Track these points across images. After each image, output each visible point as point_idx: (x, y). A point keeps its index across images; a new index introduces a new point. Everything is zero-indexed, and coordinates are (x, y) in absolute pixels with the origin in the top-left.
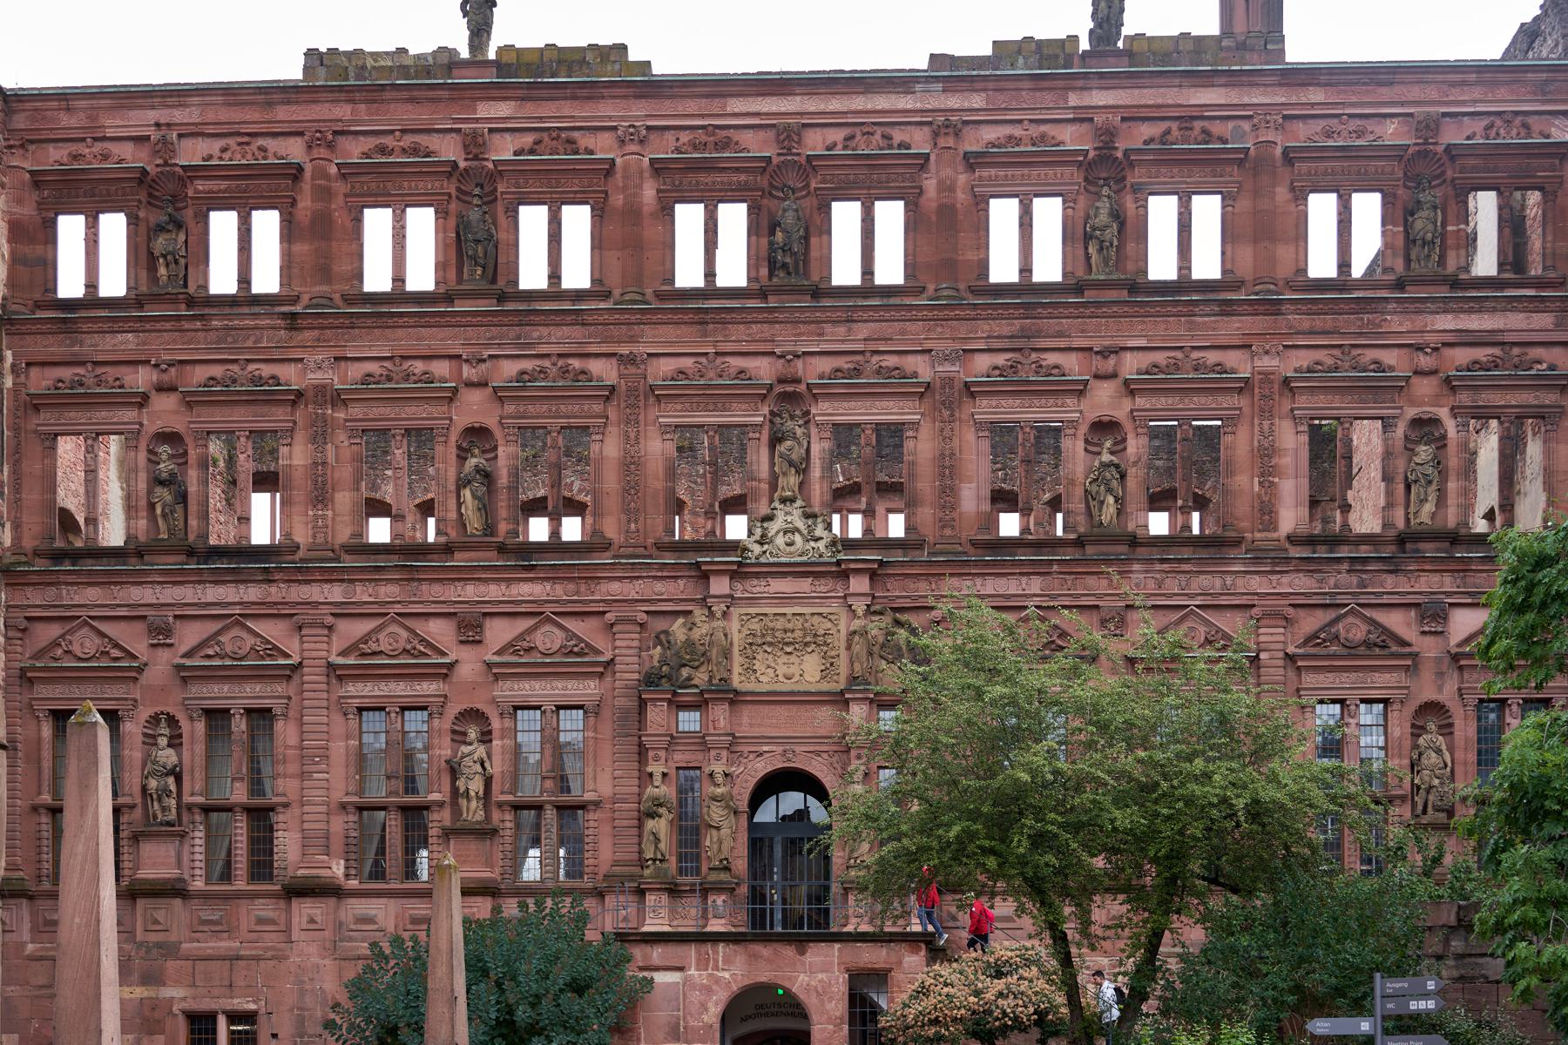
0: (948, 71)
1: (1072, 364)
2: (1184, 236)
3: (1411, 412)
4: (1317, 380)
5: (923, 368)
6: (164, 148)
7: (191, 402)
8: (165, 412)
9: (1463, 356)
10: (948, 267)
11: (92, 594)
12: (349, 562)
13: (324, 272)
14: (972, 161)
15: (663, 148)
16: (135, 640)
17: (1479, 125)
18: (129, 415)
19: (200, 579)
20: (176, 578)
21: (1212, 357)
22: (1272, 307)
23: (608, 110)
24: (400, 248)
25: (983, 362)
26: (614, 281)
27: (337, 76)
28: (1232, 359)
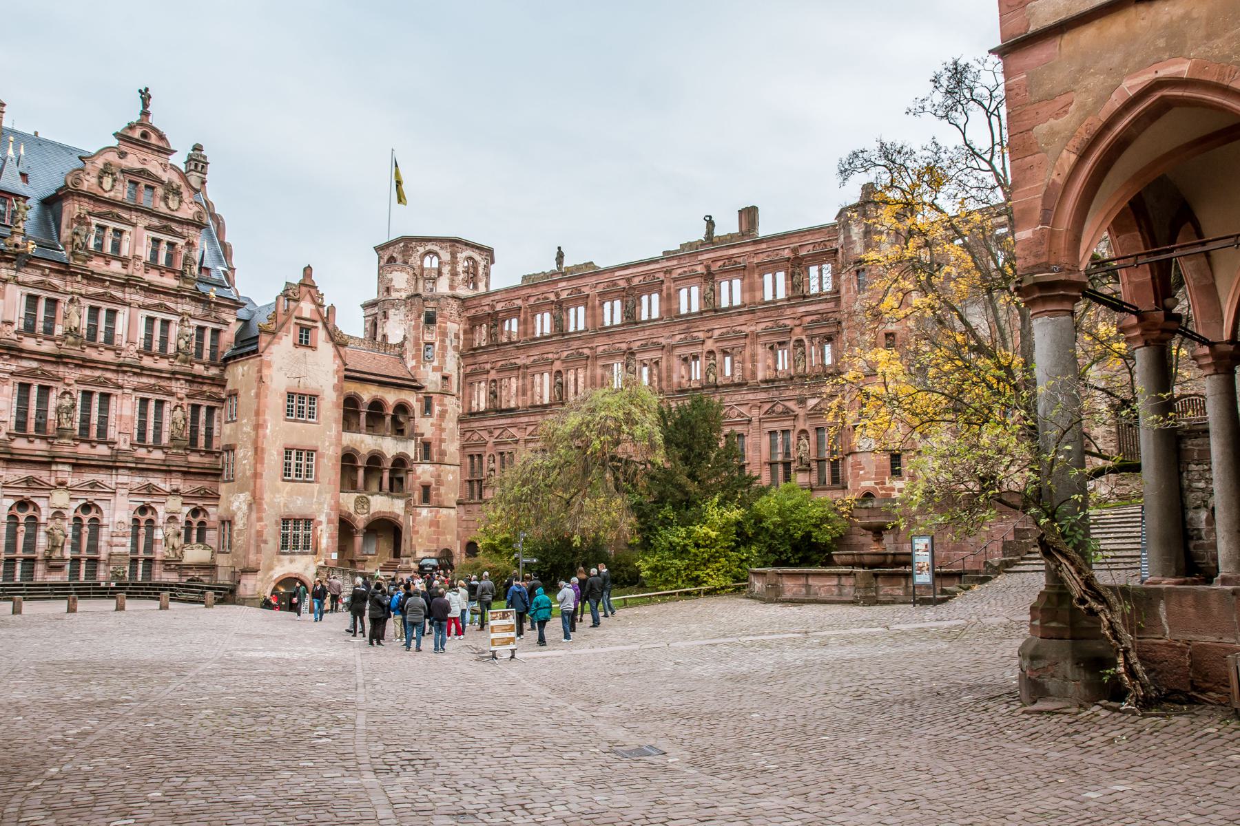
0: (669, 256)
1: (701, 335)
2: (731, 292)
3: (794, 338)
4: (766, 332)
5: (663, 341)
6: (493, 307)
7: (499, 371)
8: (493, 375)
9: (809, 319)
10: (669, 311)
11: (476, 424)
12: (531, 410)
13: (525, 334)
14: (675, 280)
15: (600, 289)
16: (485, 435)
17: (810, 247)
19: (498, 418)
20: (493, 418)
21: (738, 328)
22: (753, 312)
23: (587, 281)
24: (544, 324)
25: (678, 337)
26: (589, 327)
27: (531, 282)
28: (743, 328)
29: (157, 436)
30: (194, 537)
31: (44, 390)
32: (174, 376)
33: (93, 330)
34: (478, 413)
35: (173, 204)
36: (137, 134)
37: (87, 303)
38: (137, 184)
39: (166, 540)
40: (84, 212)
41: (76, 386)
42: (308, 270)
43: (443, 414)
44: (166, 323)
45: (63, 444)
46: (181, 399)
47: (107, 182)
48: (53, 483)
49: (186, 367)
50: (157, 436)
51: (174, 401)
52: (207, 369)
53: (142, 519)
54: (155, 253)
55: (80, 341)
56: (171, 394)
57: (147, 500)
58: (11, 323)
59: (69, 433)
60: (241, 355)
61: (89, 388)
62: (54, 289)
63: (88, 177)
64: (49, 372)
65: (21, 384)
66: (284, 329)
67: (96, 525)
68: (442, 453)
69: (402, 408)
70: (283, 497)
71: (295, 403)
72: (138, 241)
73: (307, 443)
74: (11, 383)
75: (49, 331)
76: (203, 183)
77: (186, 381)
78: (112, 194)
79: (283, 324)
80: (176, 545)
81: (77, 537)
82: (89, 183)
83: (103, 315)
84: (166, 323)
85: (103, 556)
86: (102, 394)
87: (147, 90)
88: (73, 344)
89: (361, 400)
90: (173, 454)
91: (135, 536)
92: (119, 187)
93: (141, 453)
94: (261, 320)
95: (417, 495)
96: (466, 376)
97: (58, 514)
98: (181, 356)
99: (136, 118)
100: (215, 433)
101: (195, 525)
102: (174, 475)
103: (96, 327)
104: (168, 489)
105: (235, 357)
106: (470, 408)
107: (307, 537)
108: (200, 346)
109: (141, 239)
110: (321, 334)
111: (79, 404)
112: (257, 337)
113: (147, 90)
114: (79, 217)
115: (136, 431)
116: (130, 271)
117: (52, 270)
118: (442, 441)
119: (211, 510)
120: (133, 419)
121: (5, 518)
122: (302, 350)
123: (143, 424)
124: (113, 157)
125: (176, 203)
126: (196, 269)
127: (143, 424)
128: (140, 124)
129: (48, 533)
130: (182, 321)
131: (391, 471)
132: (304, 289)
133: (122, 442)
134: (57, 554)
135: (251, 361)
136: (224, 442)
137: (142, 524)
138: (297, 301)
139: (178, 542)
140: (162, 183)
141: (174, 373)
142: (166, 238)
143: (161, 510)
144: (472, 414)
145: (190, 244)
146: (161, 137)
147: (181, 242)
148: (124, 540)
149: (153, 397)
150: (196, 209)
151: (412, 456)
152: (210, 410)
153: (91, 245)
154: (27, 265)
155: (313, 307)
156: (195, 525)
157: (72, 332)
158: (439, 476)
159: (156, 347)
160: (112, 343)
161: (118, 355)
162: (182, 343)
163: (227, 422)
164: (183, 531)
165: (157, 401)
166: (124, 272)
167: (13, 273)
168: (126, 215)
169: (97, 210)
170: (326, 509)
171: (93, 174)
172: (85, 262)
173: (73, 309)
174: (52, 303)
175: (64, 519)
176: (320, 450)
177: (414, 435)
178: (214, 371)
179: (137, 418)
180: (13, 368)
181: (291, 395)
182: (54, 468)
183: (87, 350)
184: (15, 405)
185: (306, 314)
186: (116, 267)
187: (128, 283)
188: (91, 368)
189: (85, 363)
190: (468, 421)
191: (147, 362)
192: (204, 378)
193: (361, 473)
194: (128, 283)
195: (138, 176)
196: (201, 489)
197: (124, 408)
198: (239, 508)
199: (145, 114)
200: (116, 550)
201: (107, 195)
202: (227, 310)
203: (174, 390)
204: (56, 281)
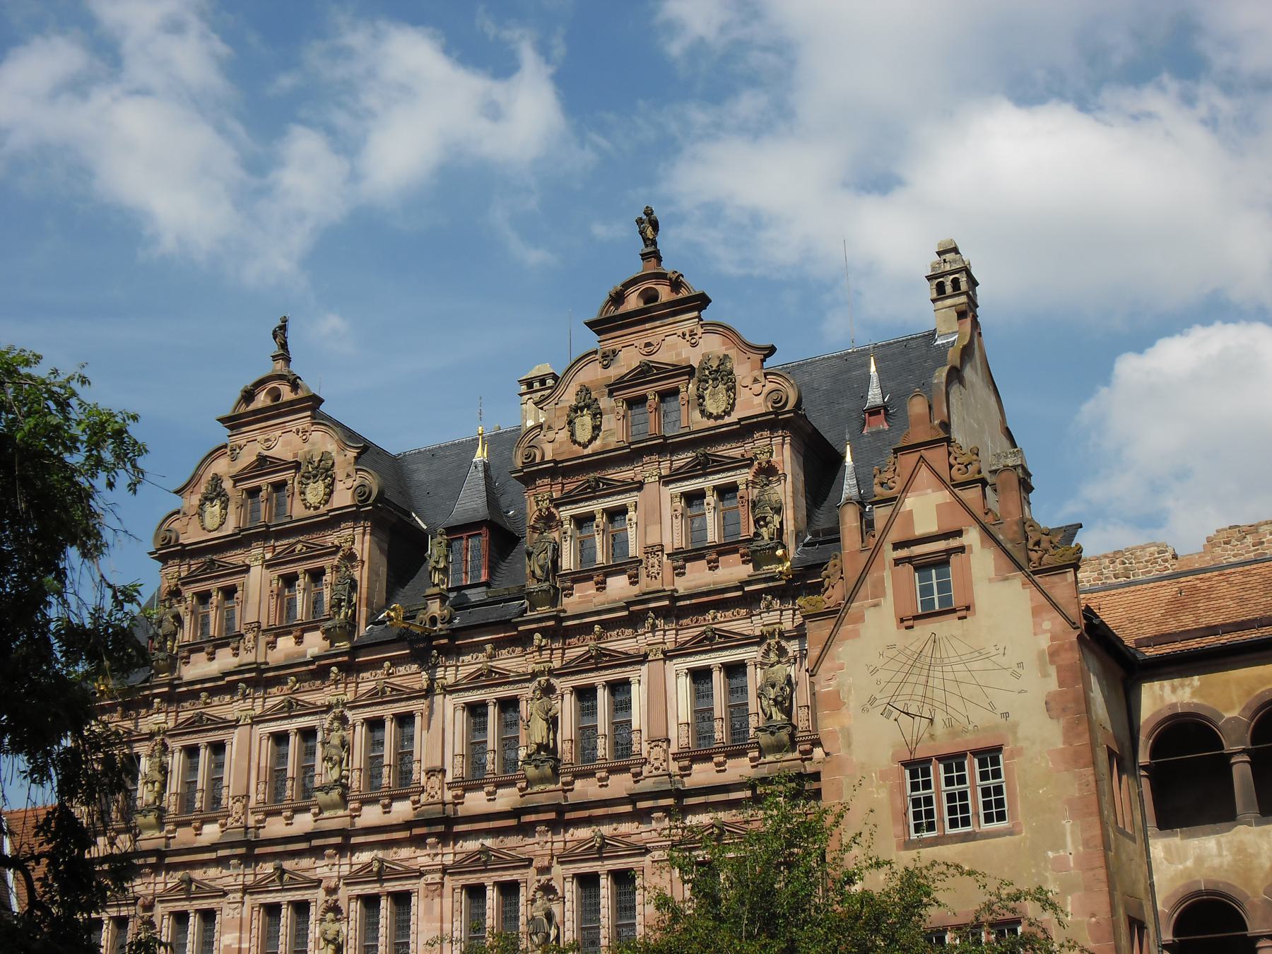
41: (557, 870)
44: (735, 670)
61: (585, 868)
63: (551, 435)
72: (656, 516)
74: (447, 890)
78: (597, 445)
87: (648, 212)
92: (609, 422)
110: (980, 560)
116: (645, 584)
140: (690, 371)
147: (741, 477)
155: (944, 496)
171: (556, 426)
172: (554, 601)
180: (449, 860)
181: (917, 768)
183: (578, 784)
185: (926, 523)
186: (619, 586)
188: (588, 822)
189: (561, 818)
191: (703, 774)
195: (650, 385)
204: (511, 662)
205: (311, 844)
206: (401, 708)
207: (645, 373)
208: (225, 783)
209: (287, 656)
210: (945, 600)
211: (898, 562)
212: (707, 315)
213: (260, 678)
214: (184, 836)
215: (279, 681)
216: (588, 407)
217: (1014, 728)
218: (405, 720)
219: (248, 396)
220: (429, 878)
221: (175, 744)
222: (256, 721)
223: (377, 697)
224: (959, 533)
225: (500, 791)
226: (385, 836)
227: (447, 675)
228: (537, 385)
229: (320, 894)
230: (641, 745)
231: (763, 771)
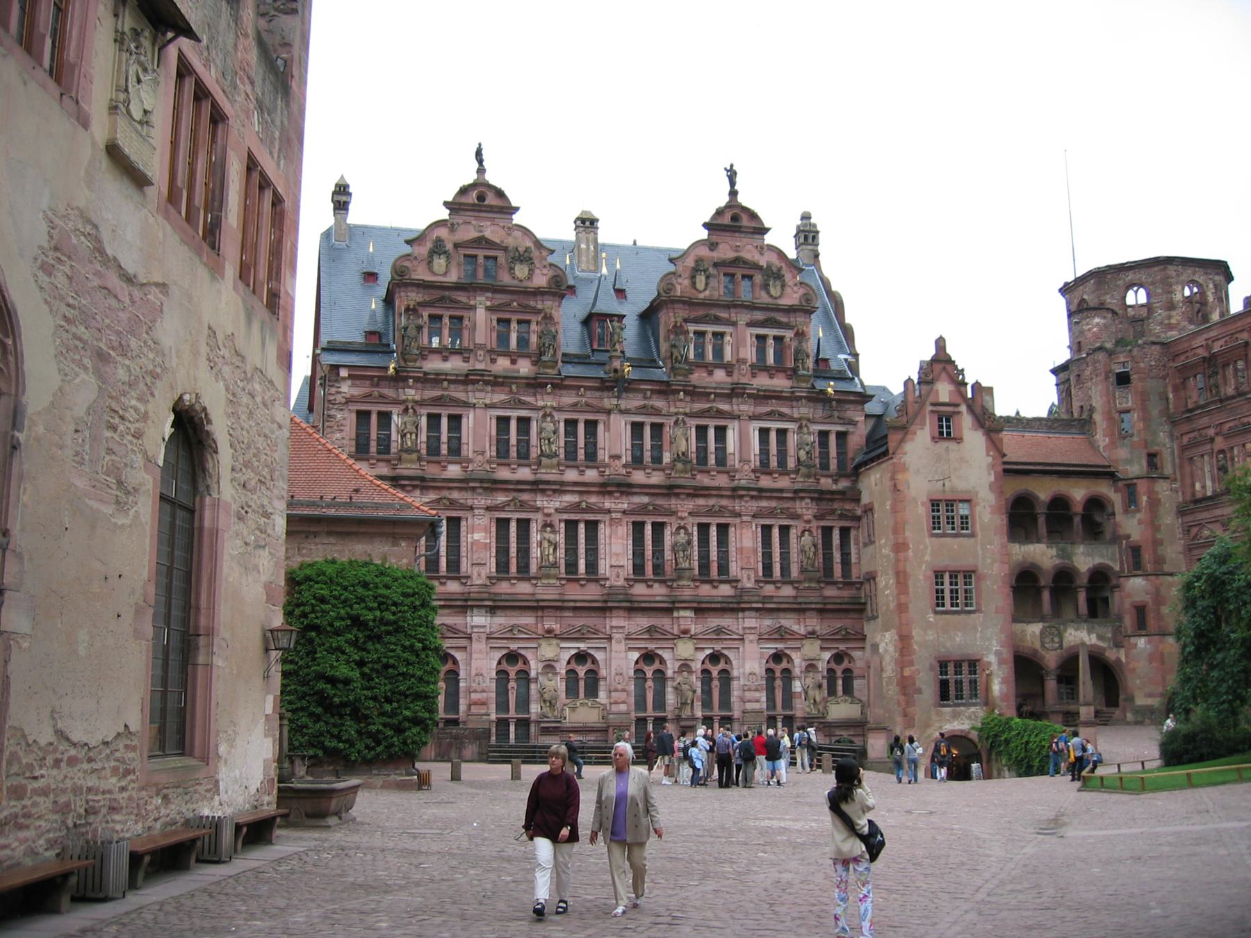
6: (1208, 348)
7: (1227, 437)
8: (1220, 443)
18: (1208, 447)
29: (785, 569)
30: (840, 688)
31: (658, 528)
32: (797, 494)
33: (702, 452)
34: (1205, 499)
35: (775, 291)
36: (726, 220)
37: (693, 423)
38: (733, 275)
39: (806, 693)
40: (680, 320)
41: (691, 519)
42: (940, 343)
43: (1154, 503)
45: (683, 587)
46: (808, 522)
47: (701, 281)
48: (676, 632)
49: (810, 483)
50: (785, 569)
51: (801, 525)
52: (835, 481)
53: (778, 669)
54: (761, 351)
55: (689, 467)
56: (796, 517)
57: (780, 646)
58: (618, 457)
59: (687, 573)
60: (872, 460)
61: (705, 520)
62: (657, 412)
63: (680, 280)
64: (661, 506)
65: (634, 523)
66: (918, 420)
67: (726, 677)
68: (1159, 561)
69: (1095, 504)
70: (937, 635)
71: (943, 513)
73: (964, 563)
75: (657, 459)
76: (817, 256)
77: (812, 499)
79: (916, 415)
80: (818, 699)
81: (707, 692)
82: (681, 287)
83: (711, 434)
84: (782, 433)
85: (736, 713)
86: (719, 525)
87: (732, 166)
88: (682, 472)
89: (1037, 498)
90: (809, 588)
91: (770, 690)
92: (713, 282)
93: (769, 589)
94: (892, 415)
95: (1128, 621)
96: (1184, 449)
97: (685, 666)
98: (803, 470)
99: (723, 200)
100: (854, 559)
101: (839, 673)
102: (808, 614)
103: (706, 449)
104: (802, 631)
105: (865, 463)
106: (1193, 494)
107: (973, 683)
108: (825, 455)
109: (744, 339)
110: (966, 420)
111: (695, 538)
112: (886, 436)
113: (732, 166)
114: (675, 326)
115: (760, 565)
116: (735, 378)
117: (651, 390)
118: (1157, 543)
119: (856, 654)
120: (755, 551)
121: (632, 673)
122: (945, 444)
123: (767, 555)
124: (704, 252)
125: (779, 288)
126: (810, 363)
127: (767, 555)
128: (728, 206)
129: (676, 688)
130: (800, 427)
131: (1088, 590)
132: (938, 367)
133: (745, 580)
134: (687, 712)
135: (884, 465)
136: (865, 568)
137: (778, 674)
138: (931, 382)
139: (818, 696)
140: (760, 268)
141: (796, 492)
142: (771, 332)
143: (797, 658)
144: (1196, 501)
145: (800, 335)
146: (753, 216)
147: (789, 334)
148: (757, 695)
149: (776, 523)
150: (802, 291)
151: (1117, 568)
152: (845, 532)
153: (692, 356)
154: (627, 390)
155: (951, 387)
156: (839, 673)
157: (681, 458)
158: (1157, 590)
159: (774, 462)
160: (725, 465)
161: (732, 478)
162: (802, 453)
163: (865, 545)
164: (825, 683)
165: (781, 527)
166: (729, 380)
167: (615, 401)
168: (724, 314)
169: (693, 315)
170: (995, 646)
172: (685, 376)
173: (679, 432)
174: (657, 429)
175: (691, 672)
176: (980, 570)
177: (1116, 539)
178: (843, 484)
179: (760, 549)
181: (935, 504)
182: (675, 614)
184: (630, 547)
186: (720, 375)
187: (735, 392)
190: (1192, 512)
191: (765, 482)
192: (833, 492)
193: (1046, 595)
194: (735, 392)
195: (735, 268)
196: (841, 629)
197: (745, 539)
198: (886, 650)
199: (733, 193)
200: (749, 706)
201: (701, 296)
202: (852, 407)
203: (799, 511)
204: (659, 403)
205: (537, 486)
206: (591, 417)
207: (737, 262)
208: (464, 440)
209: (505, 370)
210: (949, 434)
211: (932, 411)
212: (769, 239)
213: (498, 382)
214: (432, 471)
215: (502, 384)
216: (705, 271)
217: (977, 493)
218: (591, 426)
219: (464, 191)
220: (614, 515)
221: (424, 411)
222: (487, 406)
223: (574, 407)
224: (957, 405)
225: (655, 473)
226: (582, 488)
227: (624, 404)
228: (588, 224)
229: (539, 517)
230: (733, 461)
231: (798, 486)
